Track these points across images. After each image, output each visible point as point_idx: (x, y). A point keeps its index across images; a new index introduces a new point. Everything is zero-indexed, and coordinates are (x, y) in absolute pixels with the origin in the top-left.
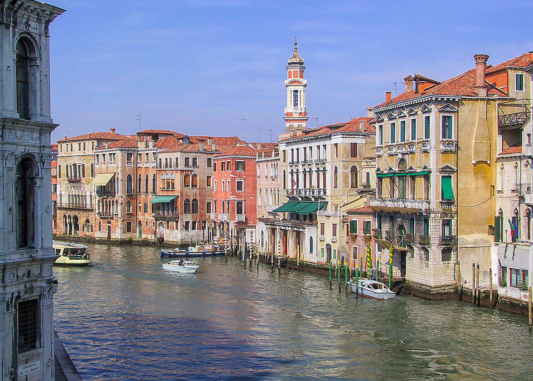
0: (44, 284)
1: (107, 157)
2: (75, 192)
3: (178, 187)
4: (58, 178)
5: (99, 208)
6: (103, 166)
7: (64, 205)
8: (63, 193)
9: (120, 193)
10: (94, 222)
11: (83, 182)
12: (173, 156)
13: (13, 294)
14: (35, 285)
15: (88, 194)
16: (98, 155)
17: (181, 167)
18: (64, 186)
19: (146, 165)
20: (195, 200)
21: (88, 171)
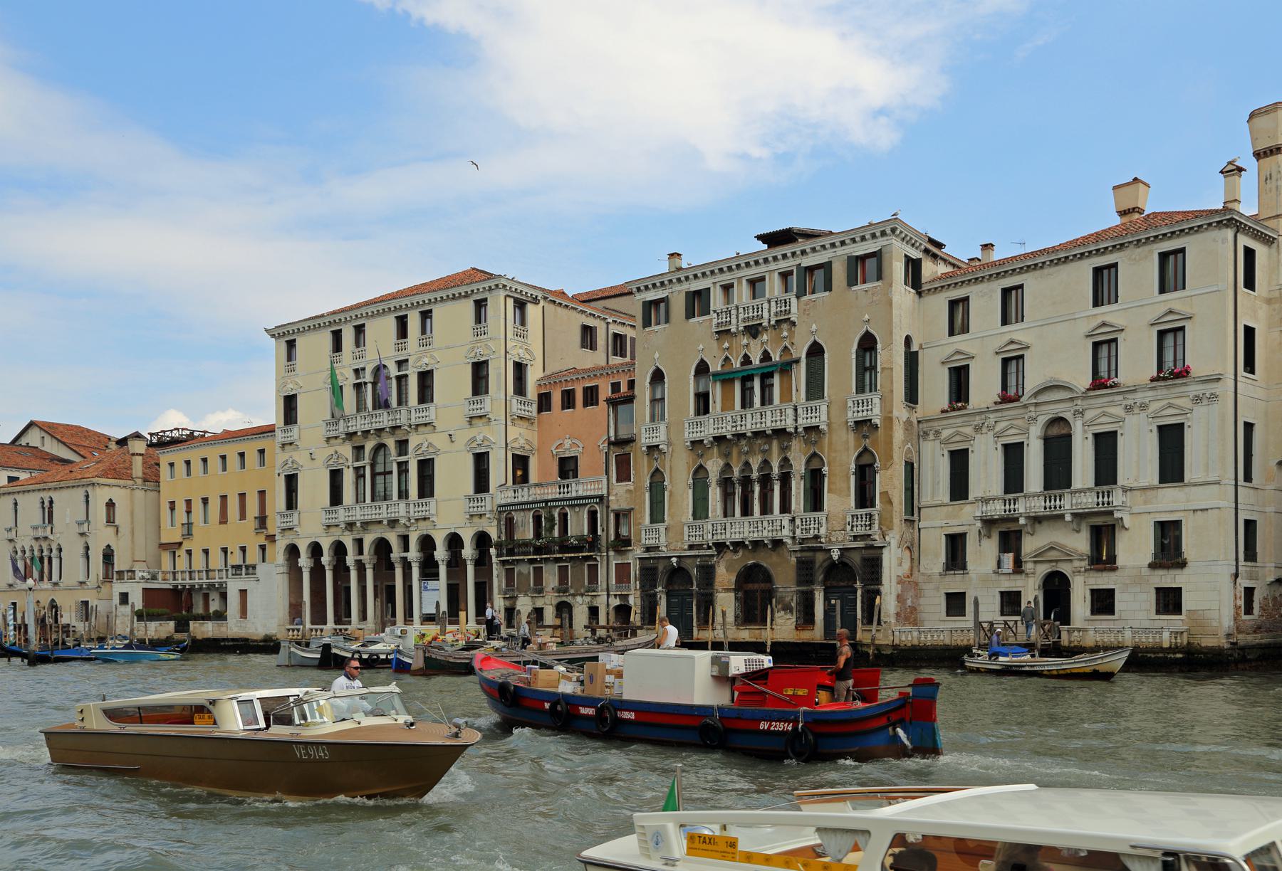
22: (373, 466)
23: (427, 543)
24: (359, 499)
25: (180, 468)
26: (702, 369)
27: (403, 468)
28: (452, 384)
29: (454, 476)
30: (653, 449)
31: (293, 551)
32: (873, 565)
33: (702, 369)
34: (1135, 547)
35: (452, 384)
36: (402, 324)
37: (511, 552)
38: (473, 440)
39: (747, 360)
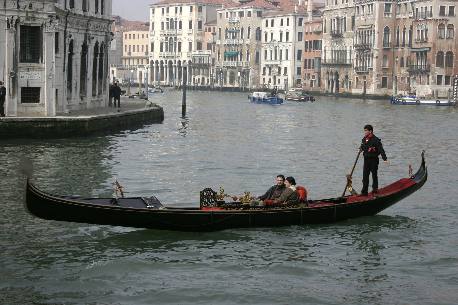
0: (45, 17)
1: (366, 8)
2: (337, 47)
3: (431, 38)
4: (324, 33)
5: (357, 64)
6: (362, 18)
7: (327, 61)
8: (327, 49)
9: (376, 46)
10: (352, 78)
11: (345, 35)
12: (428, 5)
13: (13, 17)
14: (37, 16)
15: (348, 48)
16: (358, 7)
17: (436, 15)
18: (328, 42)
19: (404, 16)
20: (450, 54)
21: (349, 24)
22: (170, 42)
23: (179, 62)
24: (166, 50)
25: (128, 36)
26: (227, 29)
27: (176, 43)
28: (186, 25)
29: (185, 47)
30: (218, 45)
31: (152, 62)
32: (248, 72)
33: (227, 29)
34: (282, 72)
35: (186, 25)
36: (176, 8)
37: (194, 66)
38: (189, 39)
39: (233, 29)
